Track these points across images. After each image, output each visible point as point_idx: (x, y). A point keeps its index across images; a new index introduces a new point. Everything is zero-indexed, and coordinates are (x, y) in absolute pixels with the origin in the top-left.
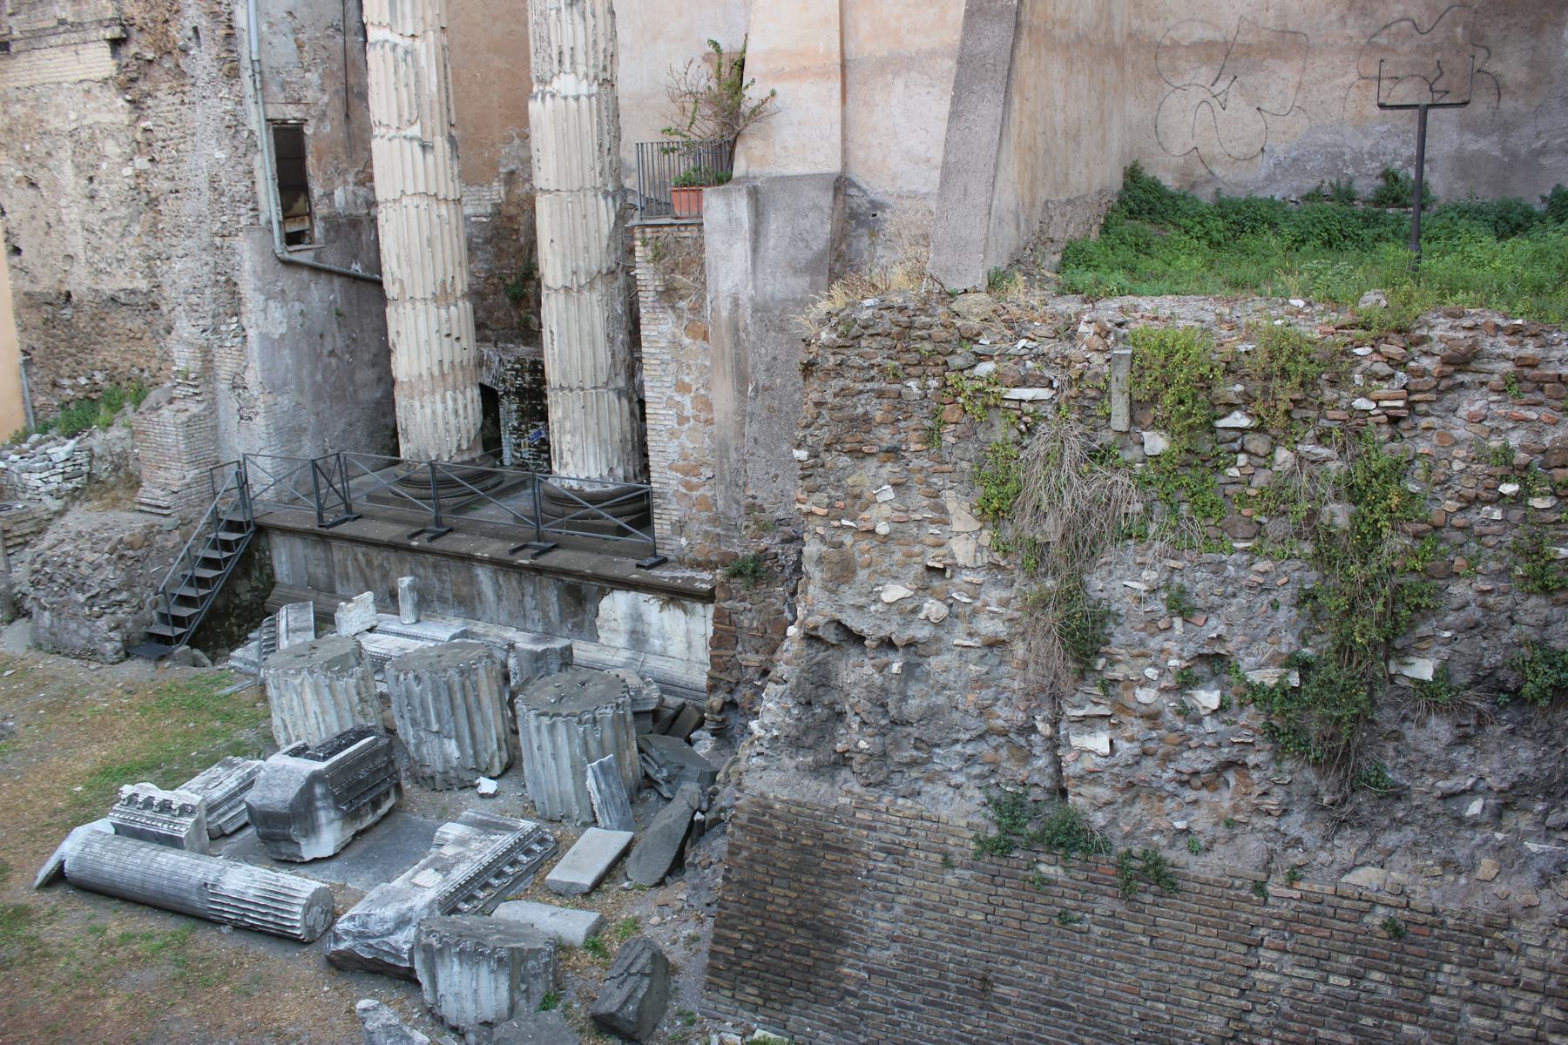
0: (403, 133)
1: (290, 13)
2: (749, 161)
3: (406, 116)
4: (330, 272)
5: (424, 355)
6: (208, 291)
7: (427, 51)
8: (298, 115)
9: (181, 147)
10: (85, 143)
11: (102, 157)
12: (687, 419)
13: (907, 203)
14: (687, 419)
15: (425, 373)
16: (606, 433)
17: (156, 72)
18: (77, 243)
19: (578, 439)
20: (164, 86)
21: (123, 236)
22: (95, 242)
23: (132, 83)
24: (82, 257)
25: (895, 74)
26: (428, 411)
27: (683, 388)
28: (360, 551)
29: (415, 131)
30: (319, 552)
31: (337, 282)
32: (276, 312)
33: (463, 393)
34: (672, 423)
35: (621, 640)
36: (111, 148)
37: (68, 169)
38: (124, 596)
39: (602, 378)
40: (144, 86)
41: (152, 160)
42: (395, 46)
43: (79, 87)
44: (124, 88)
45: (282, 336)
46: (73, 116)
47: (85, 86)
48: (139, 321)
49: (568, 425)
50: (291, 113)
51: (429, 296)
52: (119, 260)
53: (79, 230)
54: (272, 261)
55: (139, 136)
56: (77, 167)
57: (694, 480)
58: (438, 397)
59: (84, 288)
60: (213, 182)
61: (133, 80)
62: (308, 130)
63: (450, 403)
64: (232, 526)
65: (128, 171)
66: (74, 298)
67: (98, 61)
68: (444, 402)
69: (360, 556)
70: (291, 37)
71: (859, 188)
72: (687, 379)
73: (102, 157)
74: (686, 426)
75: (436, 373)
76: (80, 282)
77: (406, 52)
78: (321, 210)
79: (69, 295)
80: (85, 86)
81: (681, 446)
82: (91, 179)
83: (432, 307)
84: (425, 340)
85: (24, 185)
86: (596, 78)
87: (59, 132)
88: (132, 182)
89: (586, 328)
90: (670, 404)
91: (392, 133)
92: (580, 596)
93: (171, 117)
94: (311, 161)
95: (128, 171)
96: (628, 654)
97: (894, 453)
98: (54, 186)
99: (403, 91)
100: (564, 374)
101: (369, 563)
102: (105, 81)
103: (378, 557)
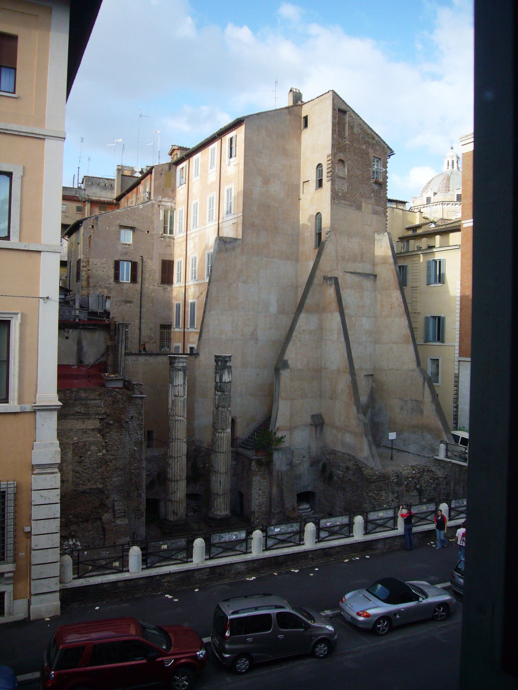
22: (78, 475)
24: (70, 480)
27: (260, 490)
40: (107, 430)
44: (100, 431)
46: (75, 439)
53: (71, 473)
55: (104, 444)
65: (101, 454)
80: (85, 430)
97: (385, 490)
102: (94, 429)
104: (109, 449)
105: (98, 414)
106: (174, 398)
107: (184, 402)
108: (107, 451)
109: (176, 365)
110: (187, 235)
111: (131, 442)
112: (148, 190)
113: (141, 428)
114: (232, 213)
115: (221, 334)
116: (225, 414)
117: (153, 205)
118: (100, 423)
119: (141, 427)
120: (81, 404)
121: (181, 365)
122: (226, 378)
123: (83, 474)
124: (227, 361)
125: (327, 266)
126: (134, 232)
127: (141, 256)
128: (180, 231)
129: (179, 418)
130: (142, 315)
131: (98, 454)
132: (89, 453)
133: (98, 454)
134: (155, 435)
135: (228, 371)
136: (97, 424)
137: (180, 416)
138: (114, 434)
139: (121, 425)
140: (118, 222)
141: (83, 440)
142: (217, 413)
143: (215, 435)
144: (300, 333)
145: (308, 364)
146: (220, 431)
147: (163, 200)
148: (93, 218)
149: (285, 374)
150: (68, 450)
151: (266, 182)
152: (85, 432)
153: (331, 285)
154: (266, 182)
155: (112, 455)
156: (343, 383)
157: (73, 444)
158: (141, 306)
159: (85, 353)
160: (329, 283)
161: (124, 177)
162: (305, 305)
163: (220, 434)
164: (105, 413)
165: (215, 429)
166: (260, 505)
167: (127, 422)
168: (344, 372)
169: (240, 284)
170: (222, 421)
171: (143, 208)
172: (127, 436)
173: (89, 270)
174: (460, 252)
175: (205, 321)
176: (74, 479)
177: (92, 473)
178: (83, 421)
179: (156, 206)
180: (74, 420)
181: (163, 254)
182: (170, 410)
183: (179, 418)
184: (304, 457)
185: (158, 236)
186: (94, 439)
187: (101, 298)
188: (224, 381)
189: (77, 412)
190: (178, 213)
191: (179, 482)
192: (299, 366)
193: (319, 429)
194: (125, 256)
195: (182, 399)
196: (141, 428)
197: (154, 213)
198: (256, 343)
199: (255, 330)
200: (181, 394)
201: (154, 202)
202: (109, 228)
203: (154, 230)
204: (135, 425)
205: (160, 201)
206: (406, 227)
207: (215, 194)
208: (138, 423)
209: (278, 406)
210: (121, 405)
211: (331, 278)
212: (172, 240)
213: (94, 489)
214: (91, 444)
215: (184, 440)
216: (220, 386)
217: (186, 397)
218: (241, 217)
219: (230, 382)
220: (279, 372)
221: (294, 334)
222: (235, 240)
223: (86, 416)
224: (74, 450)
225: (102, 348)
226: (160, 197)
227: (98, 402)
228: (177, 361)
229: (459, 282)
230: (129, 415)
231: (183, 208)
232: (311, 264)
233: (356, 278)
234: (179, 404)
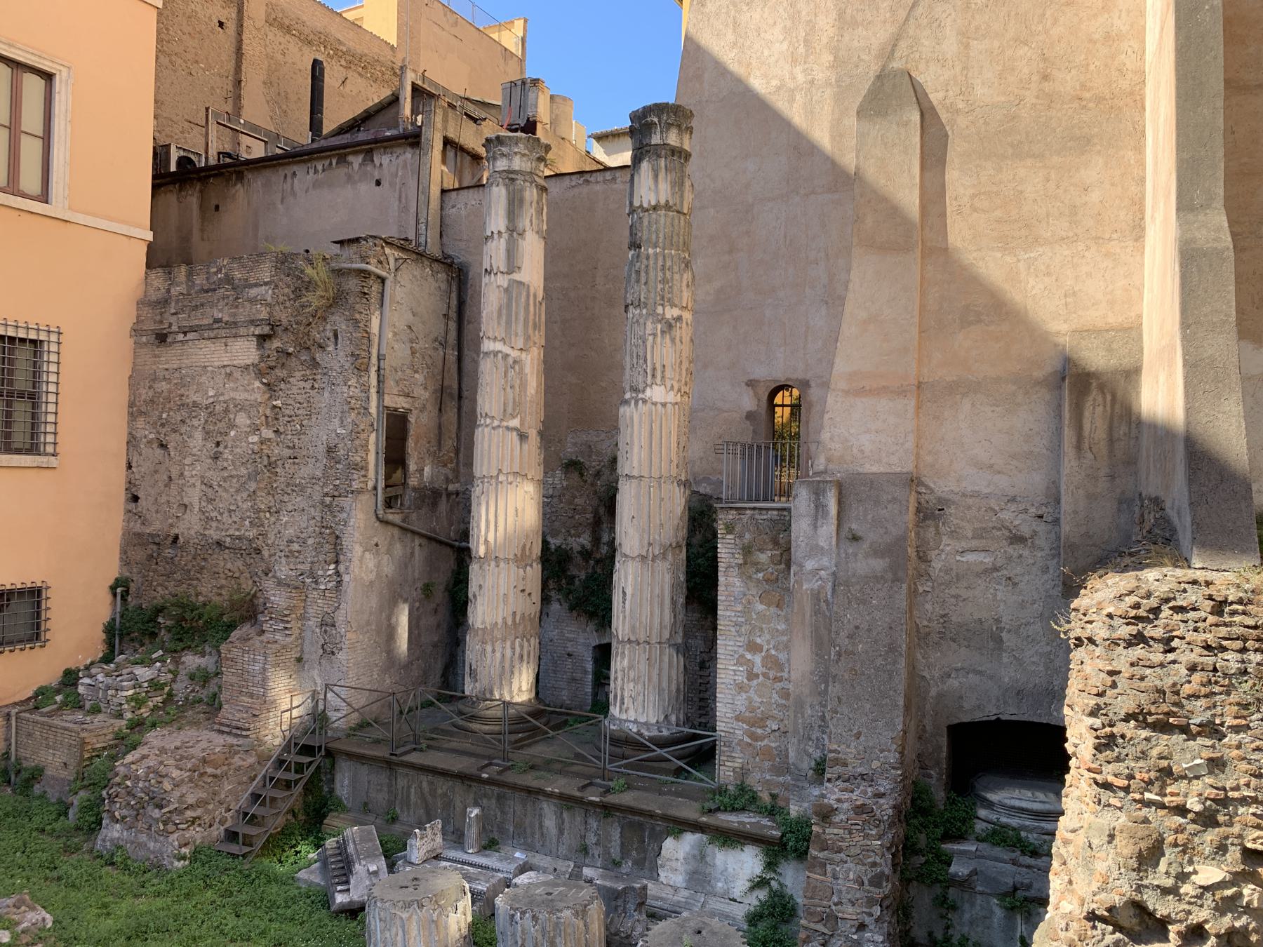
0: (505, 424)
1: (410, 327)
2: (829, 460)
3: (509, 410)
4: (413, 532)
5: (501, 605)
6: (310, 541)
7: (531, 362)
8: (405, 405)
9: (305, 423)
10: (218, 418)
11: (232, 426)
12: (757, 676)
13: (970, 501)
14: (757, 676)
15: (500, 621)
16: (665, 685)
17: (293, 362)
18: (194, 495)
19: (640, 687)
20: (298, 374)
21: (238, 491)
22: (210, 493)
23: (269, 373)
25: (964, 395)
26: (498, 655)
27: (753, 647)
28: (425, 780)
29: (515, 423)
30: (382, 777)
31: (417, 541)
32: (370, 561)
33: (528, 641)
34: (741, 678)
35: (679, 879)
36: (242, 420)
37: (199, 435)
38: (199, 812)
39: (666, 635)
40: (281, 373)
41: (276, 432)
42: (507, 355)
44: (260, 374)
45: (371, 582)
47: (228, 370)
48: (239, 563)
49: (632, 674)
50: (401, 403)
51: (512, 557)
52: (230, 511)
53: (198, 484)
54: (374, 519)
55: (268, 412)
56: (207, 433)
57: (759, 731)
58: (508, 643)
59: (192, 532)
60: (330, 450)
61: (272, 368)
62: (412, 419)
63: (518, 649)
64: (307, 750)
65: (255, 439)
66: (181, 540)
67: (245, 351)
68: (513, 648)
69: (425, 785)
70: (409, 345)
71: (927, 487)
72: (759, 641)
73: (232, 426)
74: (755, 682)
75: (510, 623)
76: (189, 526)
77: (515, 362)
78: (413, 481)
79: (176, 538)
80: (228, 370)
81: (750, 700)
82: (218, 444)
83: (513, 566)
84: (501, 594)
85: (155, 445)
86: (679, 390)
87: (195, 404)
89: (657, 591)
90: (741, 661)
91: (496, 423)
92: (645, 832)
93: (299, 399)
94: (411, 443)
95: (255, 439)
96: (686, 893)
98: (183, 448)
99: (508, 389)
100: (633, 629)
101: (433, 792)
102: (247, 367)
103: (443, 786)
104: (281, 429)
123: (220, 490)
131: (250, 440)
137: (495, 339)
141: (226, 397)
145: (1045, 77)
150: (195, 422)
152: (229, 375)
155: (289, 447)
166: (755, 721)
170: (632, 358)
176: (204, 504)
177: (238, 491)
184: (1017, 539)
186: (246, 395)
189: (218, 321)
191: (486, 567)
195: (503, 281)
213: (239, 538)
214: (240, 407)
223: (229, 329)
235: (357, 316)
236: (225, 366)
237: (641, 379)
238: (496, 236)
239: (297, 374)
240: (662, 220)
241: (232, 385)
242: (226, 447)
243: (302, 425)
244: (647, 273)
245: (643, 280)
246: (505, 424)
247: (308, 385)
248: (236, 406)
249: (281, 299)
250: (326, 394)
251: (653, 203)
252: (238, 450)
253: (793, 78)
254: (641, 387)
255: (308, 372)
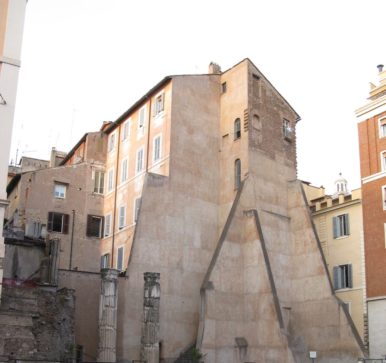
9: (50, 347)
36: (25, 345)
40: (39, 330)
43: (15, 327)
44: (32, 329)
55: (35, 343)
80: (17, 327)
88: (33, 356)
95: (32, 352)
102: (27, 327)
104: (40, 349)
105: (31, 312)
106: (105, 308)
107: (114, 313)
108: (38, 350)
109: (107, 276)
110: (116, 190)
111: (63, 344)
112: (81, 155)
113: (73, 332)
114: (160, 156)
115: (150, 260)
116: (154, 329)
117: (85, 166)
118: (33, 321)
119: (73, 330)
120: (15, 301)
121: (112, 277)
122: (155, 293)
124: (156, 278)
125: (246, 202)
126: (67, 188)
127: (73, 210)
128: (110, 188)
129: (109, 328)
130: (72, 264)
131: (30, 352)
132: (20, 350)
133: (30, 352)
134: (84, 350)
135: (157, 287)
136: (31, 323)
137: (111, 326)
138: (46, 335)
139: (53, 327)
140: (54, 178)
141: (16, 337)
142: (146, 328)
143: (143, 349)
144: (223, 259)
146: (149, 345)
147: (95, 162)
148: (31, 173)
149: (209, 294)
151: (191, 132)
152: (17, 329)
153: (251, 217)
154: (191, 132)
155: (44, 356)
156: (265, 303)
157: (6, 340)
158: (71, 255)
159: (20, 269)
160: (249, 215)
161: (57, 158)
162: (228, 234)
163: (149, 348)
164: (38, 313)
165: (144, 344)
167: (59, 324)
168: (266, 292)
169: (167, 217)
170: (150, 335)
171: (76, 168)
172: (59, 339)
173: (25, 219)
174: (361, 206)
175: (135, 247)
178: (17, 318)
179: (88, 167)
180: (7, 316)
181: (93, 210)
182: (101, 320)
183: (109, 328)
185: (89, 193)
186: (26, 337)
187: (37, 225)
188: (152, 296)
189: (11, 309)
190: (108, 173)
192: (223, 289)
193: (243, 350)
194: (58, 209)
195: (113, 309)
196: (73, 332)
197: (86, 173)
198: (182, 273)
199: (181, 260)
200: (112, 304)
201: (86, 163)
202: (45, 183)
203: (85, 188)
204: (67, 327)
205: (93, 163)
206: (311, 200)
207: (144, 147)
208: (70, 326)
209: (204, 324)
210: (54, 307)
211: (250, 211)
212: (102, 199)
215: (114, 350)
216: (149, 301)
217: (116, 308)
218: (169, 159)
219: (159, 298)
220: (205, 291)
221: (219, 258)
222: (163, 177)
223: (20, 313)
224: (5, 345)
225: (37, 265)
226: (93, 160)
227: (32, 301)
228: (109, 273)
229: (362, 232)
230: (62, 317)
231: (113, 168)
232: (231, 204)
233: (273, 218)
234: (110, 314)
235: (73, 315)
236: (15, 326)
237: (154, 341)
238: (111, 297)
239: (46, 331)
240: (158, 301)
241: (19, 333)
242: (17, 355)
243: (49, 348)
244: (155, 314)
245: (154, 315)
246: (113, 351)
247: (51, 335)
248: (21, 340)
249: (40, 305)
250: (59, 339)
251: (157, 297)
252: (23, 356)
253: (160, 264)
254: (153, 343)
255: (51, 331)
